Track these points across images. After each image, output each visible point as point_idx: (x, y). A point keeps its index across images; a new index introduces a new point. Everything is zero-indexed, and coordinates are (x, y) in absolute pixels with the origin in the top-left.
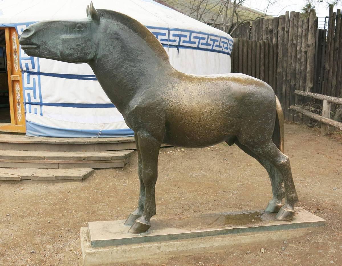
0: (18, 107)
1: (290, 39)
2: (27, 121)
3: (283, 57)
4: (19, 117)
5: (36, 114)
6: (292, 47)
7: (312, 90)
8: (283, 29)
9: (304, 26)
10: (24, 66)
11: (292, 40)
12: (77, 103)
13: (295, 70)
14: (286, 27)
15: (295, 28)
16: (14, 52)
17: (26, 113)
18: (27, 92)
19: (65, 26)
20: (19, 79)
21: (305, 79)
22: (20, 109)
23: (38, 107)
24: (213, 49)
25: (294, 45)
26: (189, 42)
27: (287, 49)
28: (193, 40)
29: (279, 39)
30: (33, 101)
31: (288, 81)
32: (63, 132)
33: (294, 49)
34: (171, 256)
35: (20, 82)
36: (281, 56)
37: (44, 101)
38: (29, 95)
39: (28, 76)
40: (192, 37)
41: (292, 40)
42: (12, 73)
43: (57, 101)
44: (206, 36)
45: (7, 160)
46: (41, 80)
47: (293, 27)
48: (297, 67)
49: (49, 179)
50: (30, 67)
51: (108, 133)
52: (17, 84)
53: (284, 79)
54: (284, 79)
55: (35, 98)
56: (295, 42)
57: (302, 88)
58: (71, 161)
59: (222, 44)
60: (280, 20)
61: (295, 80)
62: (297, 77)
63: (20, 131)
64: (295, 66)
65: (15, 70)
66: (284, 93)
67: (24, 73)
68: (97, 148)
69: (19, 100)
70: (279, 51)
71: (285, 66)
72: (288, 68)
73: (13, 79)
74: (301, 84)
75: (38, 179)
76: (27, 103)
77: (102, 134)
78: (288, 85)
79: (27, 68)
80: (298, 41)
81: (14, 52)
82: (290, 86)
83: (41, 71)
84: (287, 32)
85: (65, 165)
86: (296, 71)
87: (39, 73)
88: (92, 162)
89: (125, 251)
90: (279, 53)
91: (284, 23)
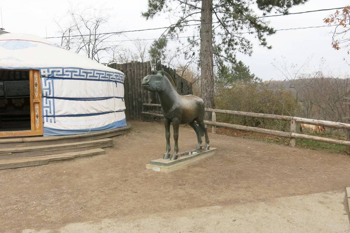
0: (37, 119)
1: (135, 76)
2: (44, 128)
3: (132, 85)
4: (38, 125)
5: (51, 122)
6: (137, 80)
7: (152, 103)
8: (131, 70)
9: (144, 70)
10: (45, 93)
11: (137, 76)
12: (75, 114)
13: (140, 93)
14: (133, 69)
15: (138, 70)
16: (35, 85)
17: (44, 123)
18: (45, 109)
19: (156, 77)
20: (39, 101)
21: (147, 98)
22: (38, 121)
23: (52, 118)
24: (87, 78)
25: (139, 79)
26: (94, 76)
27: (134, 81)
28: (95, 75)
29: (128, 75)
30: (49, 114)
31: (137, 99)
32: (70, 132)
33: (139, 81)
34: (188, 166)
35: (40, 103)
36: (131, 85)
37: (56, 114)
38: (47, 111)
39: (46, 99)
40: (95, 73)
41: (137, 76)
42: (34, 98)
43: (64, 114)
44: (104, 73)
45: (55, 150)
46: (68, 101)
47: (137, 70)
48: (142, 91)
49: (89, 155)
50: (48, 94)
51: (96, 130)
52: (37, 104)
53: (134, 97)
54: (134, 97)
55: (50, 113)
56: (139, 78)
57: (146, 102)
58: (91, 145)
59: (120, 78)
60: (128, 65)
61: (141, 98)
62: (142, 96)
63: (38, 134)
64: (140, 90)
65: (36, 96)
66: (135, 106)
67: (43, 98)
68: (93, 138)
69: (37, 115)
70: (129, 82)
71: (134, 90)
72: (136, 92)
73: (35, 102)
74: (145, 100)
75: (83, 156)
76: (45, 116)
77: (91, 131)
78: (136, 101)
79: (47, 95)
80: (141, 77)
81: (35, 85)
82: (138, 102)
83: (55, 96)
84: (133, 72)
85: (88, 148)
86: (141, 93)
87: (53, 98)
88: (100, 144)
89: (177, 166)
90: (129, 83)
91: (131, 67)
